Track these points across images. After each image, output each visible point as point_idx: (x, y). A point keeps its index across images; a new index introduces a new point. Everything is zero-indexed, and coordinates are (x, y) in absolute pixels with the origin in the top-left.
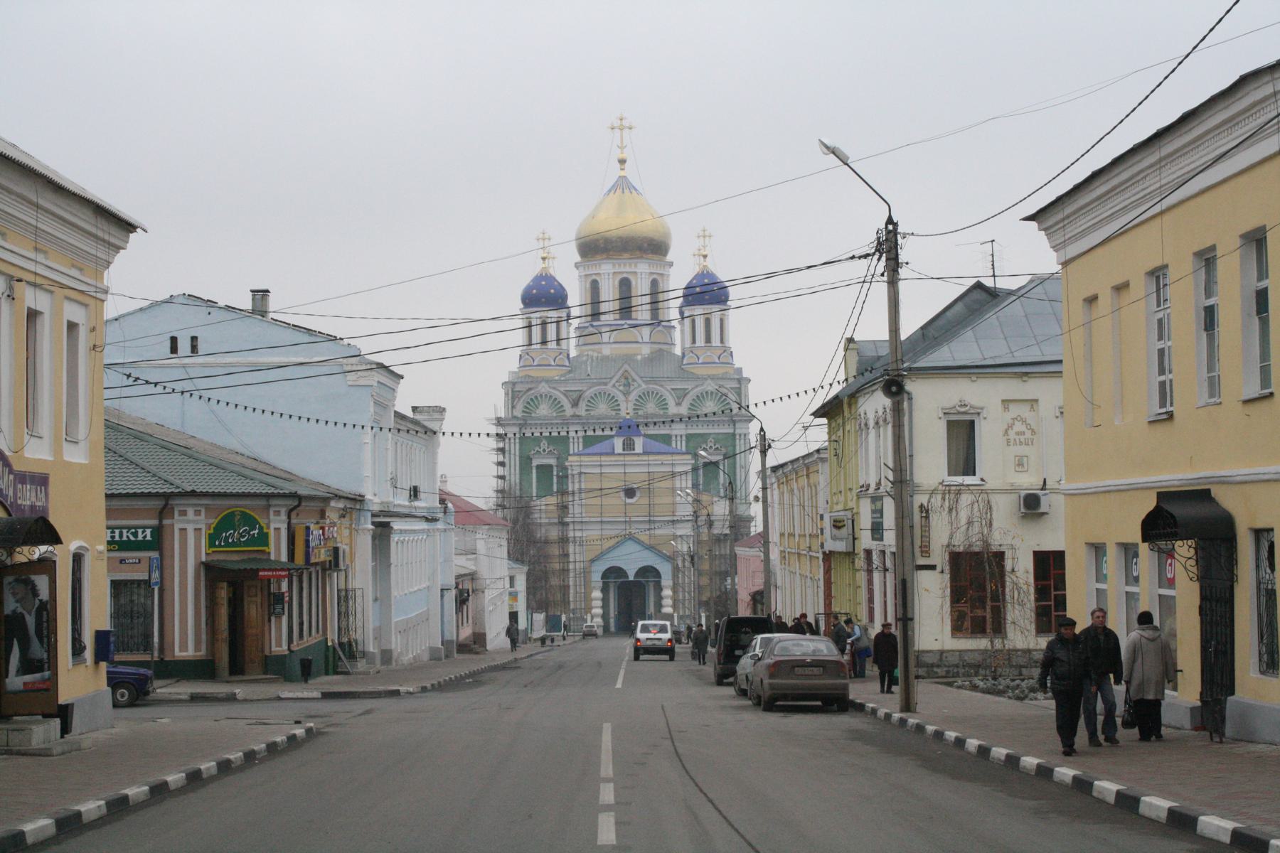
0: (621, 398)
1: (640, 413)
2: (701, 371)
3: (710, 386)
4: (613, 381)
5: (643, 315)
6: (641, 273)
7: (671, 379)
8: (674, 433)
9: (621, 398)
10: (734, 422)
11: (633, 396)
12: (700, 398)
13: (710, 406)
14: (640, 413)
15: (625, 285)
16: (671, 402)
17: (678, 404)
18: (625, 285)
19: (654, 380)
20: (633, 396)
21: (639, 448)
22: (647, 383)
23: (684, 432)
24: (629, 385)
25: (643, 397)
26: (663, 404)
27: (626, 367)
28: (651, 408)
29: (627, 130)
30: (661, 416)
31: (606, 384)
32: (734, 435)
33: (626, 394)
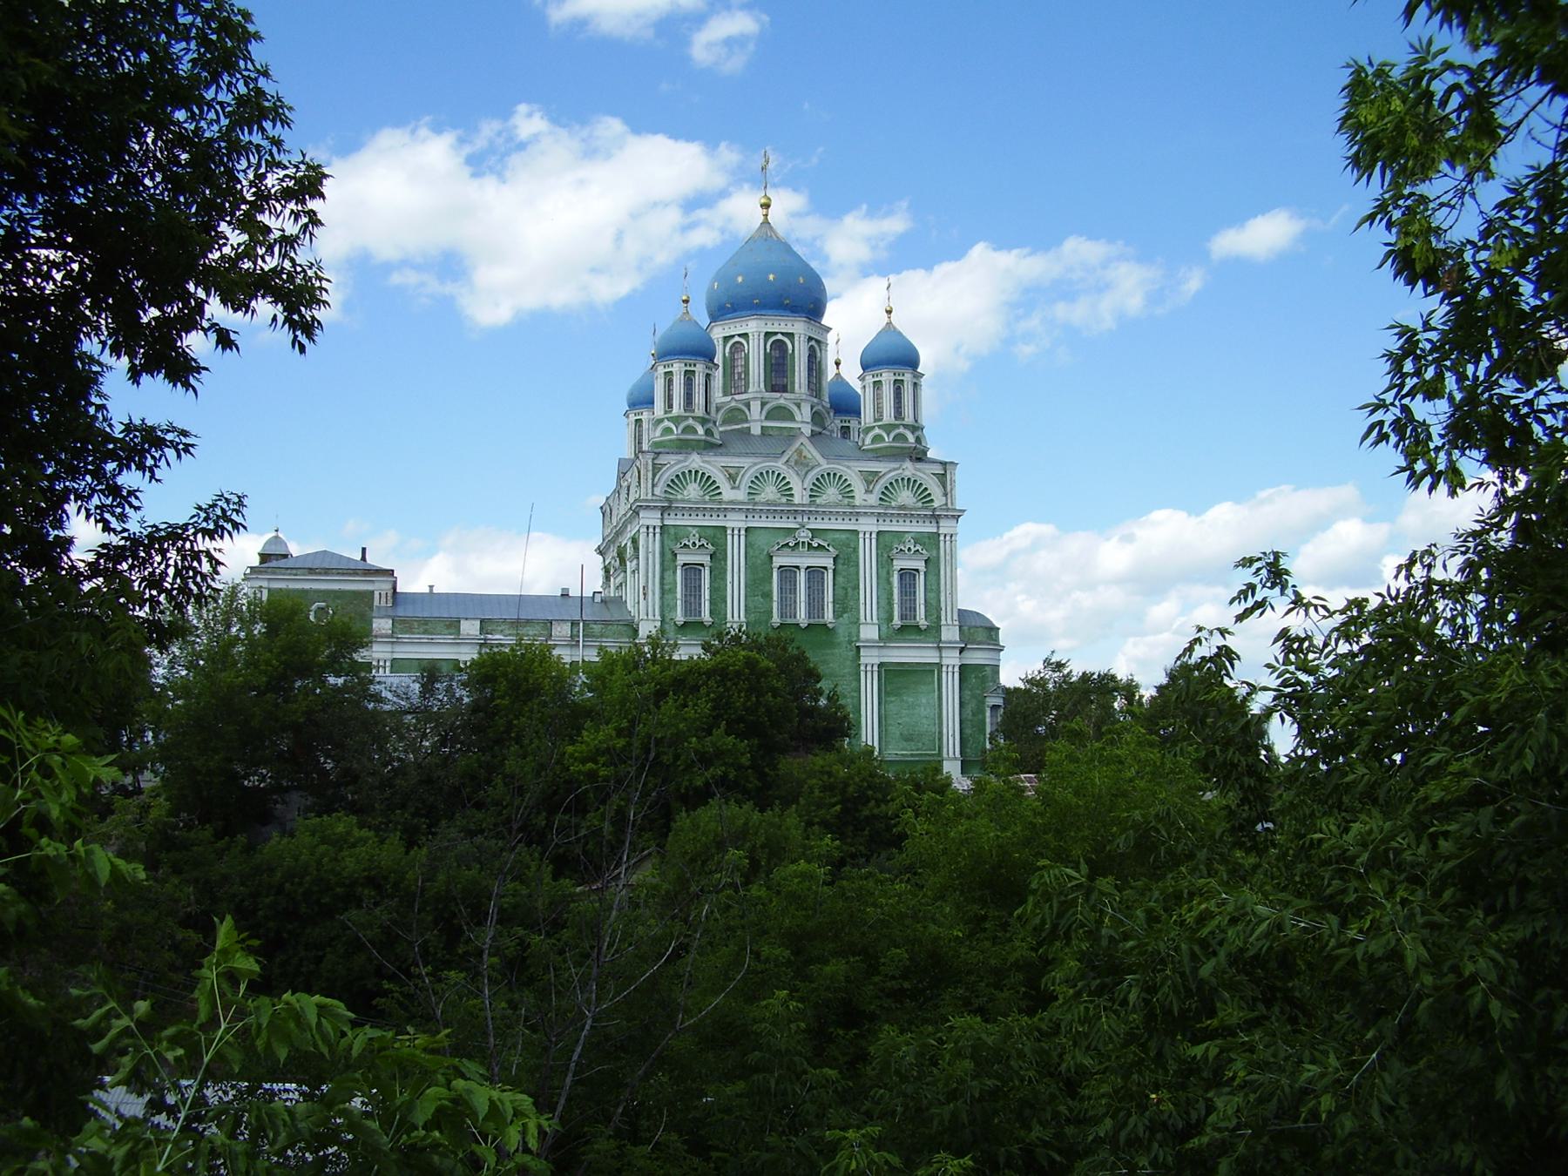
26: (847, 493)
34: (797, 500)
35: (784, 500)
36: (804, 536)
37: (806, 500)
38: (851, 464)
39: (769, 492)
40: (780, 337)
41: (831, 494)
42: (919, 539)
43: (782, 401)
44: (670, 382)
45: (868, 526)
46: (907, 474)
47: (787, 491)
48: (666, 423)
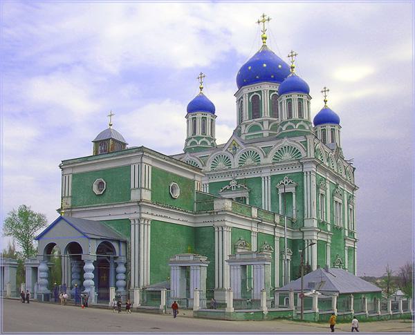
0: (231, 156)
1: (243, 165)
8: (263, 175)
9: (231, 156)
16: (261, 155)
25: (244, 156)
26: (257, 159)
33: (233, 155)
34: (232, 167)
35: (227, 167)
36: (233, 184)
37: (237, 165)
38: (256, 144)
39: (221, 165)
40: (255, 94)
41: (249, 161)
42: (291, 176)
43: (254, 123)
44: (195, 121)
45: (266, 173)
46: (286, 144)
47: (228, 161)
48: (193, 140)
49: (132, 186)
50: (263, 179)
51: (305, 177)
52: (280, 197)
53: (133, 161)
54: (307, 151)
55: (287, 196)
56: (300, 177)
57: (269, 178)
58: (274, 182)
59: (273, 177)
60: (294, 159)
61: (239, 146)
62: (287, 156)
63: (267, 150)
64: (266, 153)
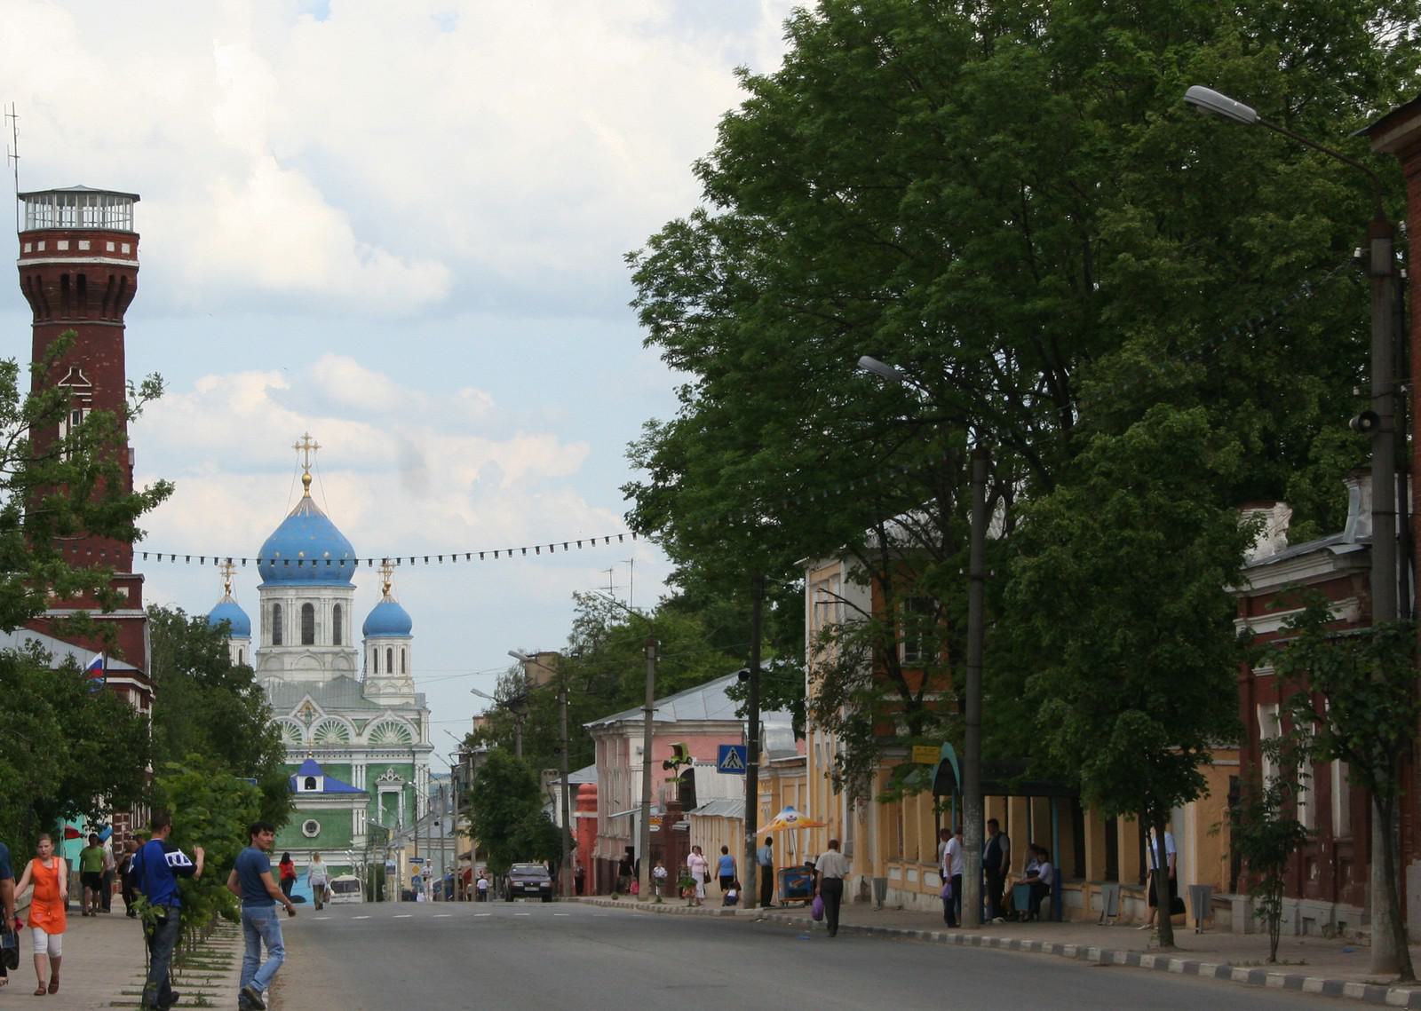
1: (321, 742)
2: (383, 702)
3: (389, 716)
4: (294, 712)
5: (324, 636)
6: (324, 599)
7: (352, 709)
8: (354, 762)
10: (414, 753)
11: (316, 724)
12: (380, 728)
13: (391, 737)
14: (321, 742)
15: (308, 610)
16: (352, 732)
17: (359, 735)
18: (308, 610)
19: (335, 710)
20: (316, 724)
21: (320, 787)
22: (328, 713)
23: (364, 762)
24: (309, 715)
26: (345, 736)
27: (308, 697)
28: (332, 737)
29: (312, 449)
30: (342, 746)
31: (287, 714)
32: (413, 765)
33: (308, 725)
34: (304, 743)
40: (308, 601)
42: (398, 769)
45: (359, 760)
49: (355, 832)
50: (354, 768)
51: (417, 772)
52: (380, 798)
53: (356, 805)
54: (420, 734)
55: (390, 797)
56: (410, 771)
57: (364, 768)
58: (370, 774)
59: (369, 767)
60: (400, 742)
61: (315, 710)
62: (391, 737)
63: (361, 725)
64: (359, 729)
